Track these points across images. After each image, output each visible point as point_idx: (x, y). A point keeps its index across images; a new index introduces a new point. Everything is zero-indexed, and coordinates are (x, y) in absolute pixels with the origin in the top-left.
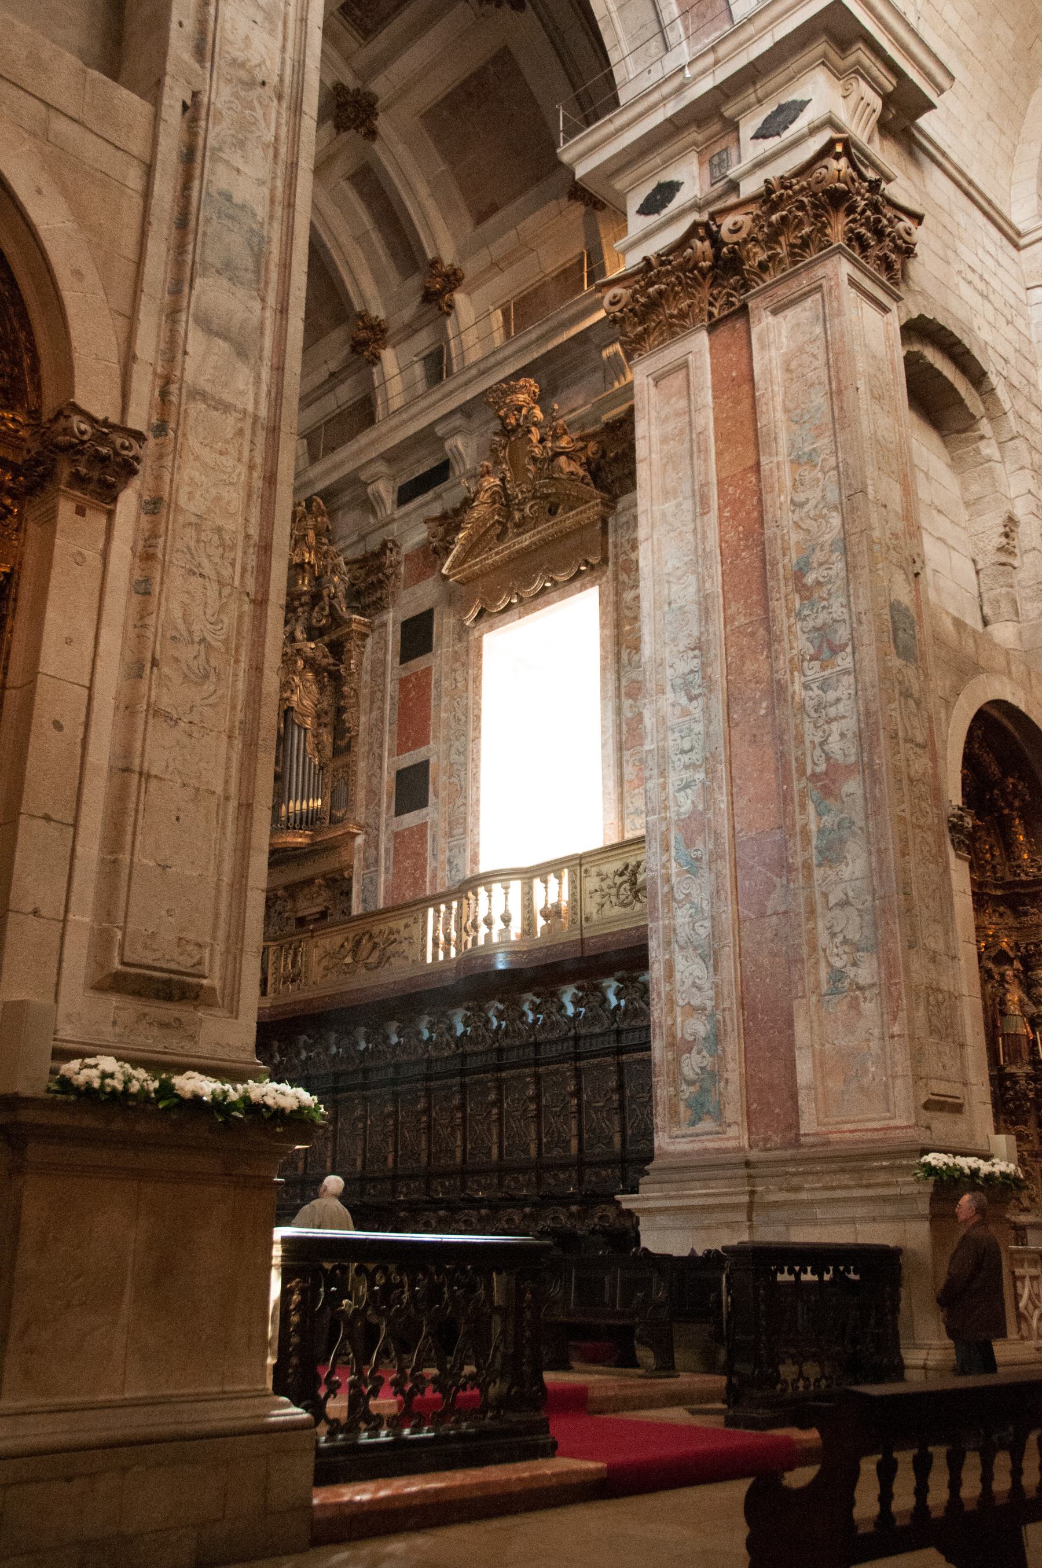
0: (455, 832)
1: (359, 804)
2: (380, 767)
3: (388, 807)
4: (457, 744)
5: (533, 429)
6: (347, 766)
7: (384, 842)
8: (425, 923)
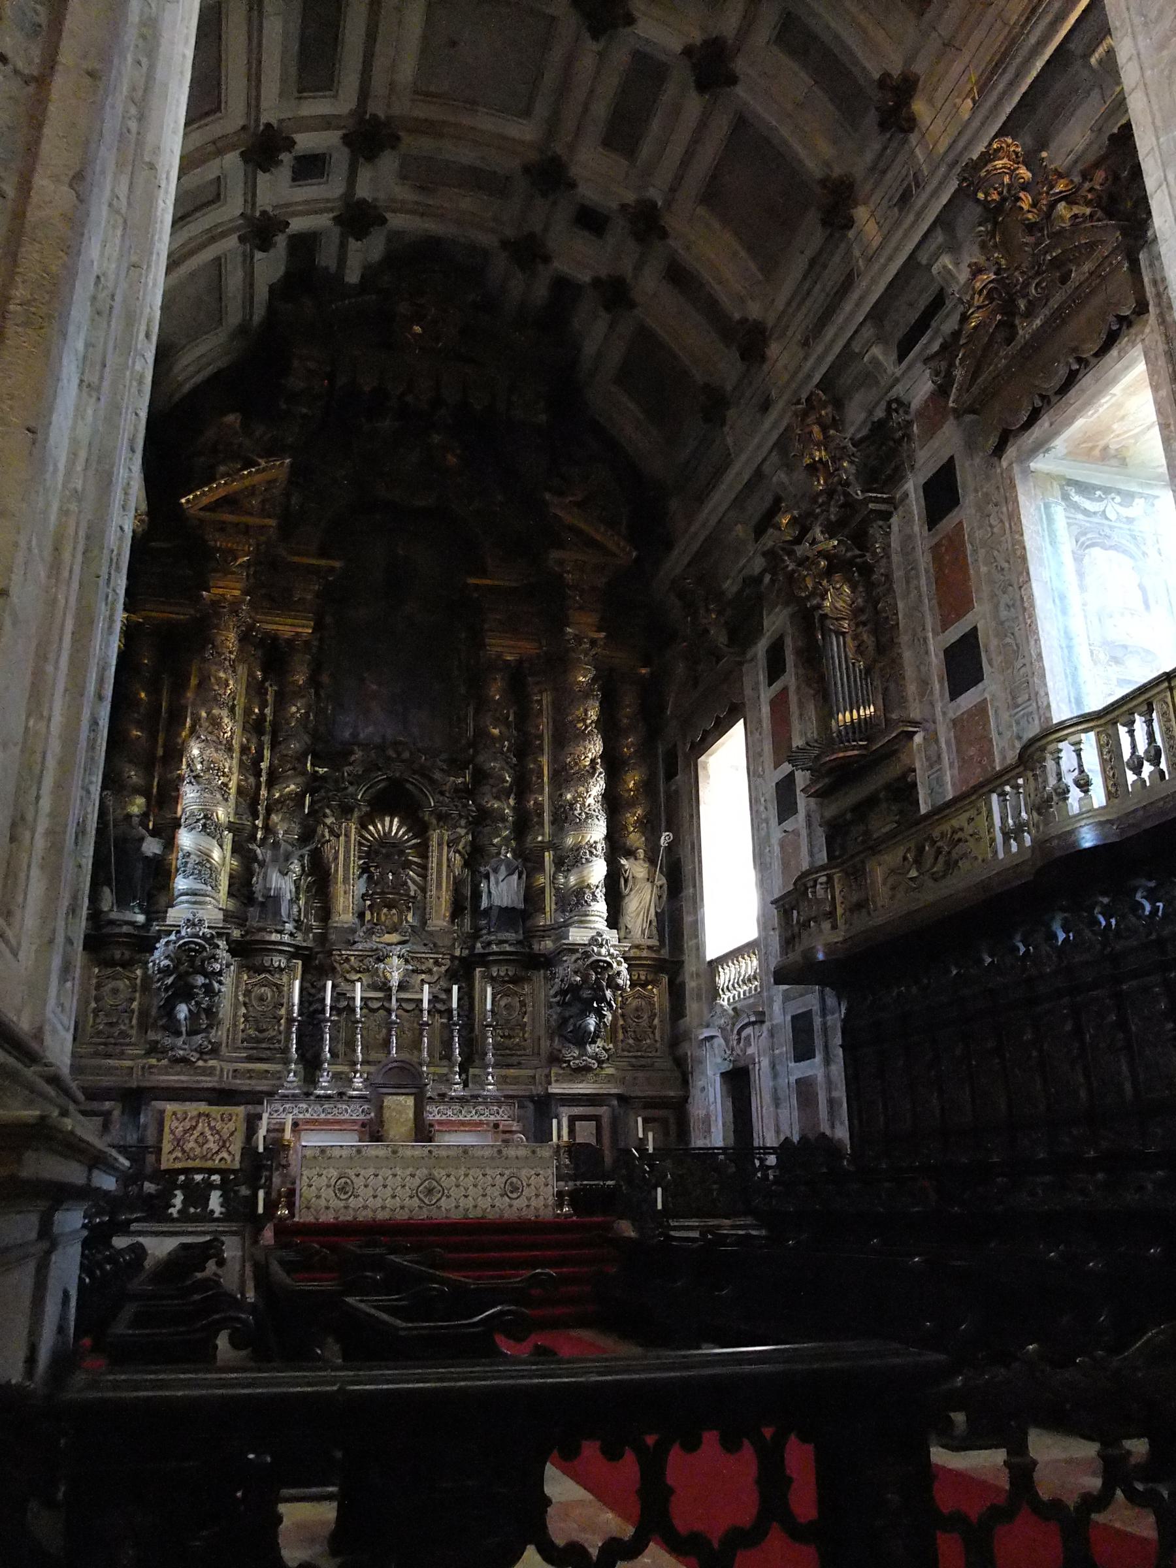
0: (1020, 700)
1: (911, 699)
2: (927, 652)
3: (942, 695)
4: (1005, 599)
5: (1022, 195)
6: (893, 661)
7: (944, 733)
8: (990, 811)
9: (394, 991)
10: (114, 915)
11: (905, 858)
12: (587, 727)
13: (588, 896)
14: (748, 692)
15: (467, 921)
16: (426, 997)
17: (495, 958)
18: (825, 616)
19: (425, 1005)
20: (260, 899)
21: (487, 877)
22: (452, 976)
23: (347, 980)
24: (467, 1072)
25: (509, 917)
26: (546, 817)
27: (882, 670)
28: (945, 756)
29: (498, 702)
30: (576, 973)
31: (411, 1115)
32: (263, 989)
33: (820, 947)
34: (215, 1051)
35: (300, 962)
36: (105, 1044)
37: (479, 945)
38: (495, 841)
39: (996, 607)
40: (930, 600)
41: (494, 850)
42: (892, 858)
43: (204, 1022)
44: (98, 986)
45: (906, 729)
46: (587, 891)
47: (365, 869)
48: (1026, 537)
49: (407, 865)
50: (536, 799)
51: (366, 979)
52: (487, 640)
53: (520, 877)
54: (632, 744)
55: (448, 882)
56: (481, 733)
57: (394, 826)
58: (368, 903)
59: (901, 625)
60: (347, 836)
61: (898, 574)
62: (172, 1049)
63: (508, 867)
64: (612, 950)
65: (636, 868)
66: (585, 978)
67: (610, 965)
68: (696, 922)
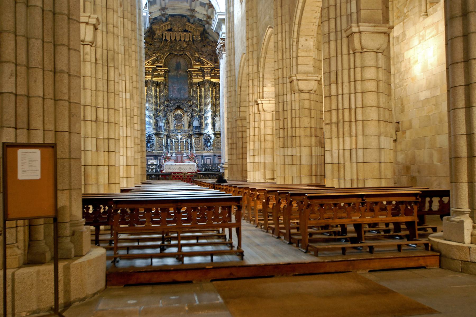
13: (208, 125)
19: (185, 142)
22: (189, 137)
25: (196, 128)
26: (203, 111)
34: (154, 150)
35: (165, 136)
43: (152, 146)
49: (181, 119)
56: (193, 96)
57: (179, 112)
66: (207, 138)
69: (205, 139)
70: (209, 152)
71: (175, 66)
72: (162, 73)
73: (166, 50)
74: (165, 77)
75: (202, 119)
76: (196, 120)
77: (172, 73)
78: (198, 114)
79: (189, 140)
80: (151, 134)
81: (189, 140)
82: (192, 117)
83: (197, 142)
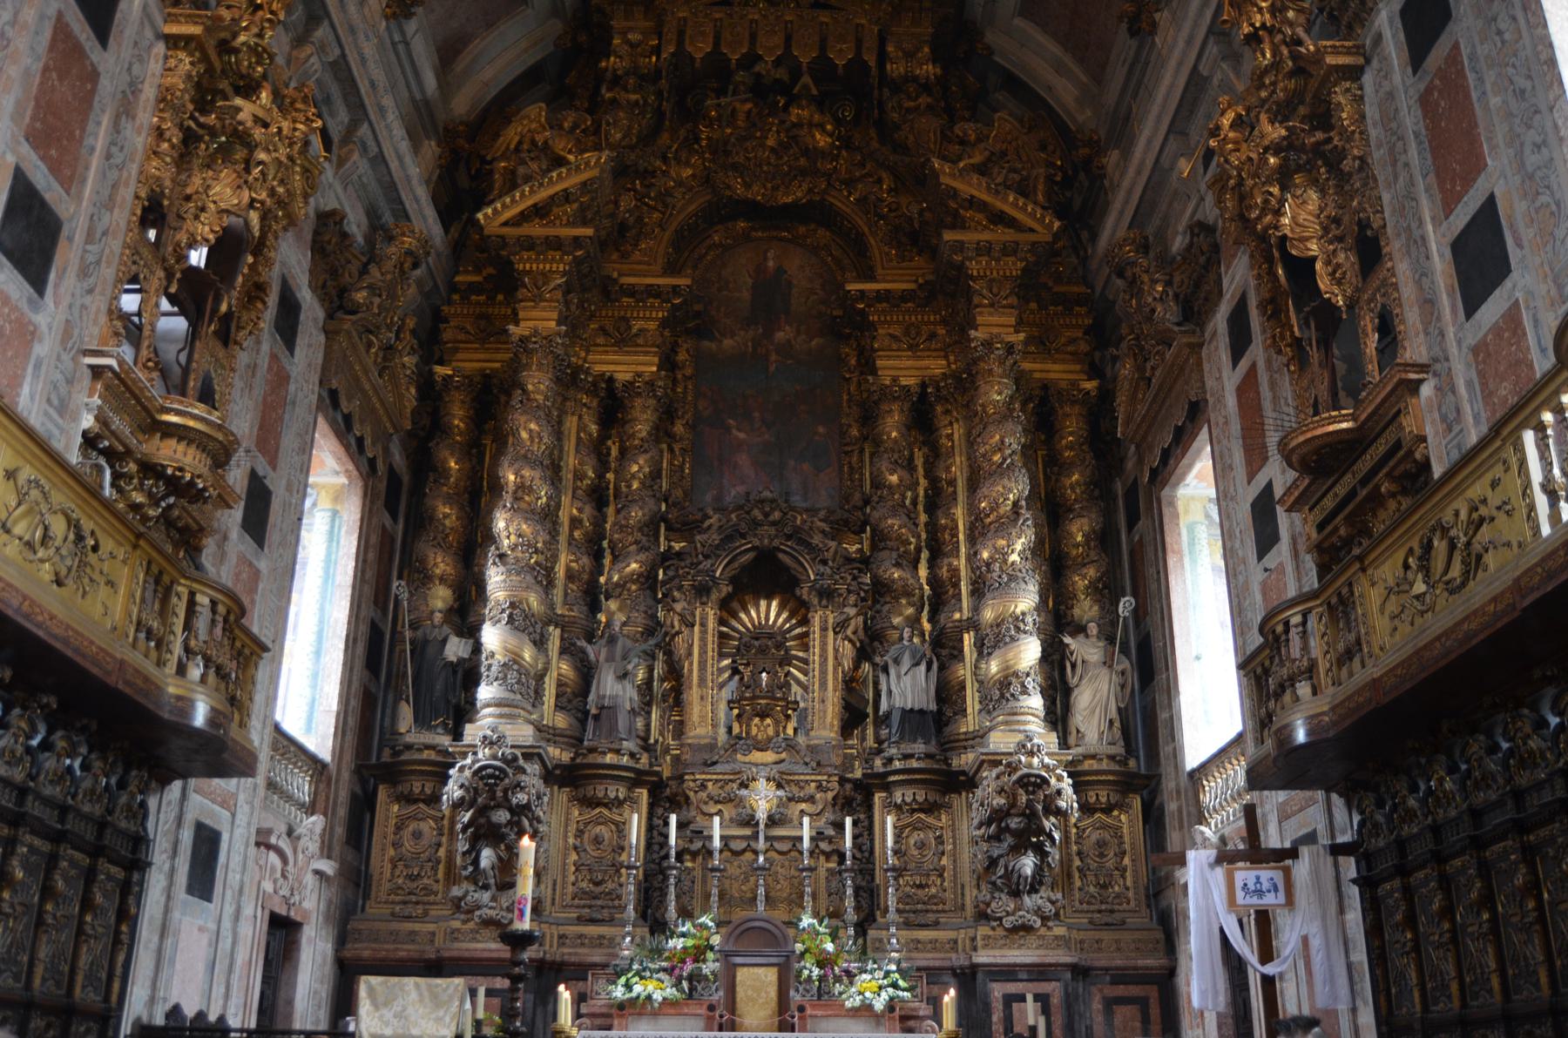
7: (1462, 371)
8: (1523, 463)
9: (762, 826)
10: (410, 738)
11: (1406, 567)
12: (1005, 460)
13: (1015, 688)
14: (1210, 383)
15: (870, 731)
16: (806, 833)
17: (901, 777)
18: (1285, 237)
20: (594, 711)
21: (886, 670)
22: (844, 804)
23: (705, 814)
24: (864, 934)
25: (914, 721)
26: (964, 588)
27: (1372, 299)
28: (1467, 408)
29: (895, 441)
30: (1001, 791)
31: (773, 992)
32: (598, 829)
33: (1299, 722)
35: (645, 792)
36: (405, 903)
37: (878, 762)
38: (897, 621)
39: (1520, 154)
40: (1425, 176)
41: (895, 635)
42: (1388, 571)
44: (399, 828)
45: (1403, 376)
46: (1014, 680)
47: (735, 671)
48: (1553, 28)
49: (787, 660)
50: (950, 565)
51: (729, 811)
52: (879, 363)
53: (929, 669)
54: (1077, 482)
55: (835, 678)
56: (878, 484)
57: (769, 613)
58: (736, 711)
59: (1389, 230)
60: (703, 625)
61: (1378, 155)
62: (479, 908)
63: (913, 656)
64: (1047, 760)
65: (1087, 650)
67: (1045, 782)
68: (1171, 717)
69: (997, 816)
70: (1031, 939)
71: (746, 295)
72: (648, 321)
73: (690, 172)
74: (668, 363)
75: (958, 655)
76: (906, 662)
77: (728, 343)
78: (918, 620)
79: (848, 821)
80: (508, 751)
81: (848, 821)
82: (870, 645)
83: (921, 846)
